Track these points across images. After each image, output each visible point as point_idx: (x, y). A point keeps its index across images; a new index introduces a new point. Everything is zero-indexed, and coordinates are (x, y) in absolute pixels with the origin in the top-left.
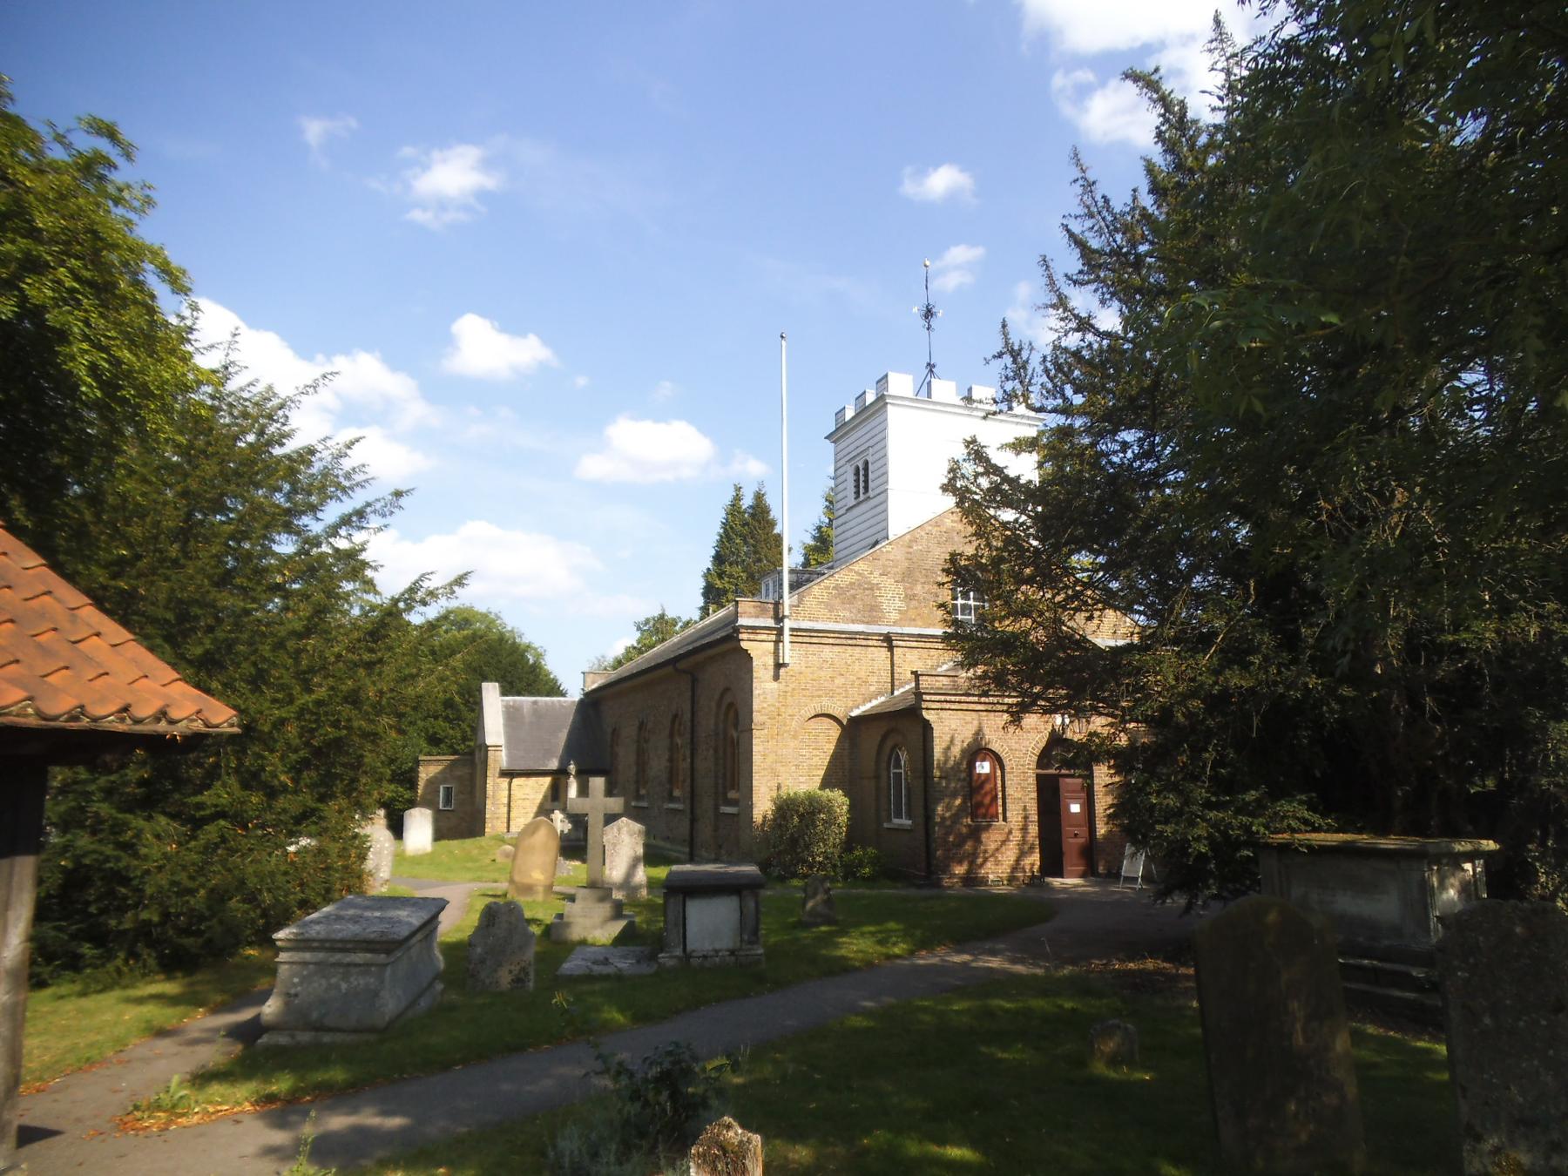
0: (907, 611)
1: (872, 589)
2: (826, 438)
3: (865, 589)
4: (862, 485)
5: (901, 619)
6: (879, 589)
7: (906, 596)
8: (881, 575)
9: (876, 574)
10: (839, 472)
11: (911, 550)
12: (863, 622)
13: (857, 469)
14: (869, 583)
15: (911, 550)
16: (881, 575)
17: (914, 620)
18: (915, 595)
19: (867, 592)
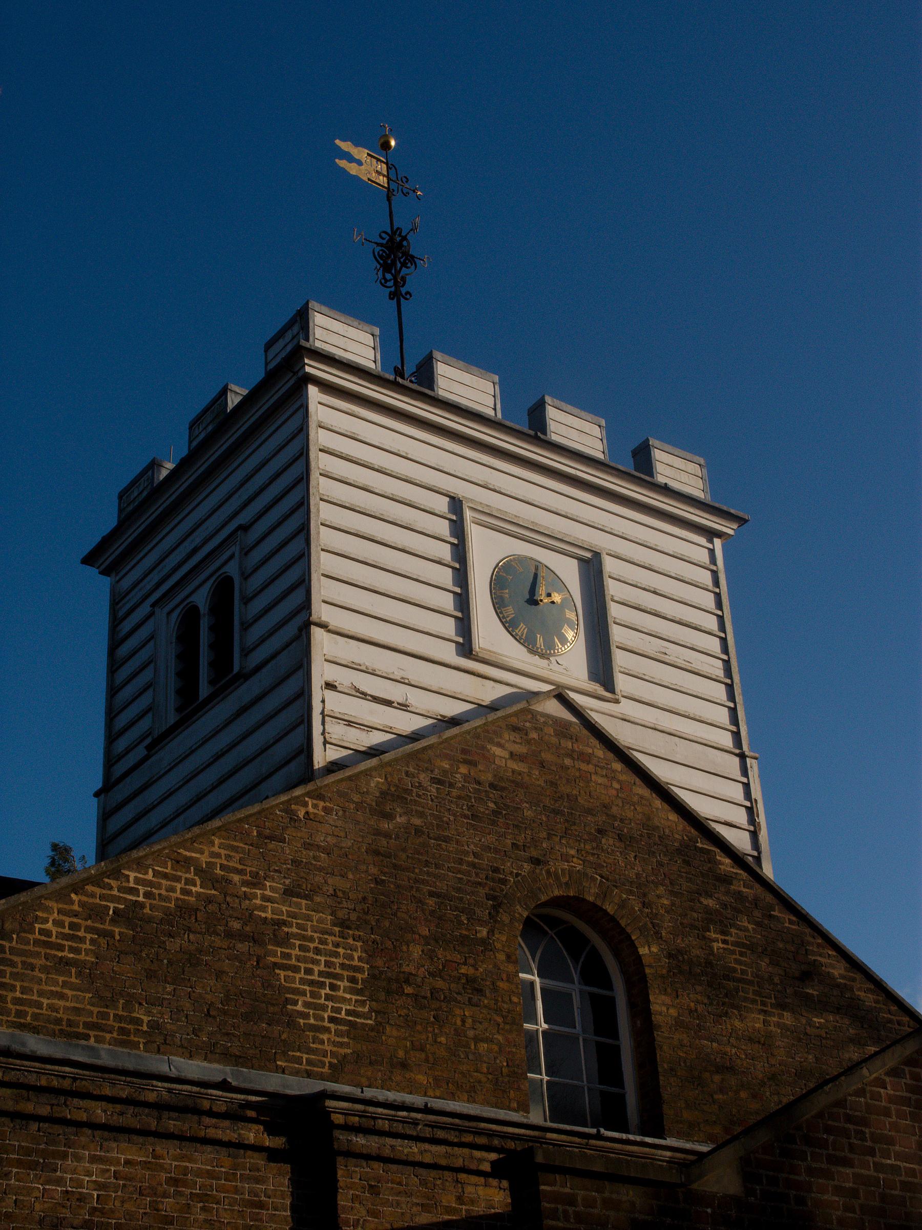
0: (378, 1028)
1: (255, 939)
2: (89, 560)
3: (229, 934)
4: (205, 656)
5: (358, 1057)
6: (284, 941)
7: (373, 976)
8: (289, 892)
9: (273, 887)
10: (124, 650)
11: (385, 825)
12: (226, 1057)
13: (191, 616)
14: (249, 917)
15: (385, 825)
16: (289, 892)
17: (404, 1065)
18: (408, 979)
19: (243, 947)
